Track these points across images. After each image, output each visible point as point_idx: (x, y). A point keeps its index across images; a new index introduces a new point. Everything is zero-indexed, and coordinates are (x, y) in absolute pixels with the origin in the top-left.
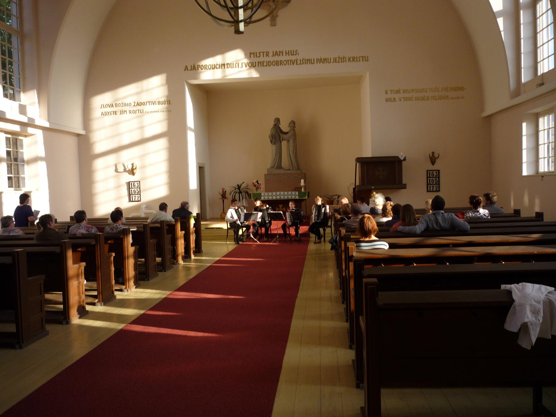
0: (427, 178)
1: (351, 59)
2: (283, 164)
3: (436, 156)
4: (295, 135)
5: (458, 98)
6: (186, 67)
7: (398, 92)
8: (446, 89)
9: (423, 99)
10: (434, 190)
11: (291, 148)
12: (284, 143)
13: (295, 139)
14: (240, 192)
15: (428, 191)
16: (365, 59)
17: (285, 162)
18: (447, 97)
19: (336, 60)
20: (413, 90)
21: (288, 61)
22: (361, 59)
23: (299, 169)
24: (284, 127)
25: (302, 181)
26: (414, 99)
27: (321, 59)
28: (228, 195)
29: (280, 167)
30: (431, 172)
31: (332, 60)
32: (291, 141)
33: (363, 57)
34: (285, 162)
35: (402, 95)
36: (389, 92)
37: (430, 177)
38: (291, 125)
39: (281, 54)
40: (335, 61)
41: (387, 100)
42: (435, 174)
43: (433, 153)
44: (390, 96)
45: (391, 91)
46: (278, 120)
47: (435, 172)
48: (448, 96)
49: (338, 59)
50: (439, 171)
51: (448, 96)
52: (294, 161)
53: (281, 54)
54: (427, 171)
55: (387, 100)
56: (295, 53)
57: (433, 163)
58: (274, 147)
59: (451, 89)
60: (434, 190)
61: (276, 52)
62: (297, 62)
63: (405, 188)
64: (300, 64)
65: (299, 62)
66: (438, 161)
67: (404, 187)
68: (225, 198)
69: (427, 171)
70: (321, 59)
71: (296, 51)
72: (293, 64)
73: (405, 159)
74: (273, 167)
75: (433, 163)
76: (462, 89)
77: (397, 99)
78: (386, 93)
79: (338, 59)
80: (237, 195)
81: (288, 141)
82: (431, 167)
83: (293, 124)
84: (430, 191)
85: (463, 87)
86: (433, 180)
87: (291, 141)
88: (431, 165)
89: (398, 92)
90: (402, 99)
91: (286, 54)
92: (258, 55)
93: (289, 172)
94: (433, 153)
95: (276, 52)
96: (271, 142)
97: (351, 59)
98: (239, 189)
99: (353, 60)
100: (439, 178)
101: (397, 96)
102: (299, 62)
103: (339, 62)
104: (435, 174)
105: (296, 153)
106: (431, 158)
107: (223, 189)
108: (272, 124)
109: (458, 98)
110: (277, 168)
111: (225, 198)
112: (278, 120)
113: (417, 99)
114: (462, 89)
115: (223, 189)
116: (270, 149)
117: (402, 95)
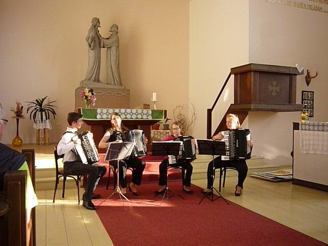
2: (102, 77)
3: (312, 75)
11: (113, 58)
14: (42, 110)
18: (319, 9)
23: (121, 85)
24: (104, 32)
29: (97, 80)
32: (114, 48)
38: (113, 29)
42: (310, 95)
46: (96, 23)
48: (321, 8)
50: (313, 92)
51: (321, 8)
52: (116, 75)
54: (303, 92)
57: (308, 83)
58: (92, 53)
68: (21, 117)
69: (303, 92)
75: (308, 83)
80: (39, 114)
82: (306, 88)
83: (115, 29)
87: (114, 48)
88: (306, 85)
93: (110, 87)
96: (90, 46)
98: (41, 105)
104: (310, 95)
105: (118, 64)
107: (18, 104)
108: (89, 25)
110: (94, 81)
111: (21, 117)
112: (96, 23)
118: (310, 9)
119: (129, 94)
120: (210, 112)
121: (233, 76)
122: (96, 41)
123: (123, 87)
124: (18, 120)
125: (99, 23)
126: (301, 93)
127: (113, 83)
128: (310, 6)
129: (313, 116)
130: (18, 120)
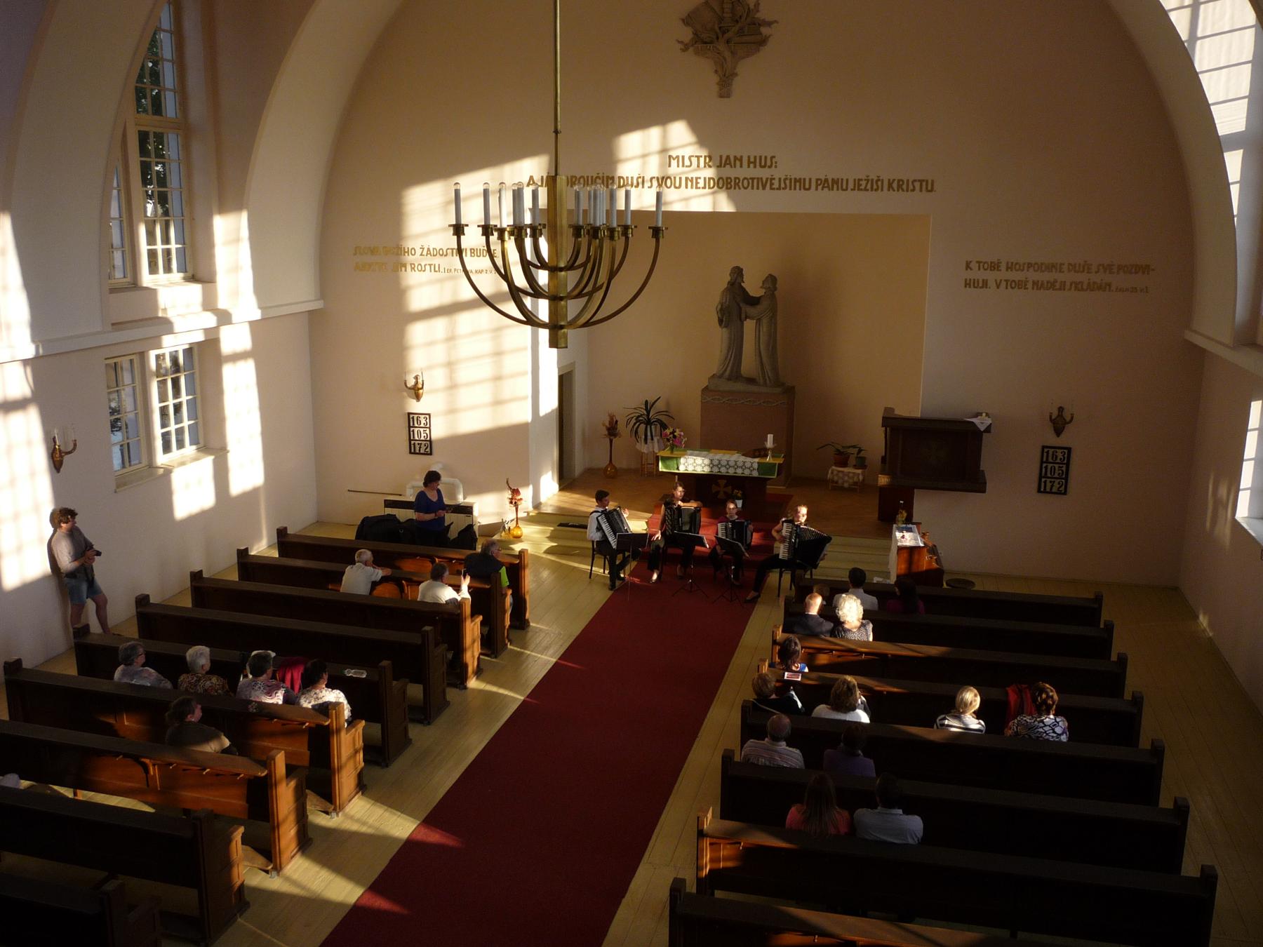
0: (1042, 462)
1: (895, 185)
4: (773, 310)
5: (1134, 290)
6: (531, 178)
7: (994, 266)
8: (1108, 268)
9: (1051, 285)
10: (1054, 490)
11: (763, 338)
12: (749, 325)
15: (1039, 491)
16: (927, 186)
17: (749, 364)
19: (860, 185)
20: (1030, 265)
21: (753, 179)
22: (917, 185)
24: (753, 286)
25: (770, 437)
26: (1030, 285)
27: (826, 180)
28: (621, 427)
30: (1051, 451)
31: (851, 185)
32: (765, 321)
33: (921, 181)
34: (749, 364)
35: (1003, 274)
36: (974, 265)
37: (1047, 462)
39: (738, 163)
40: (857, 186)
41: (967, 284)
43: (1061, 409)
44: (976, 274)
45: (979, 262)
46: (738, 272)
49: (863, 183)
50: (1069, 450)
51: (1110, 285)
52: (768, 367)
53: (738, 163)
54: (1044, 447)
55: (967, 284)
56: (769, 163)
57: (1058, 432)
59: (1120, 268)
60: (1054, 490)
61: (728, 157)
62: (772, 184)
64: (779, 189)
65: (776, 185)
66: (1069, 429)
68: (615, 435)
69: (1044, 447)
70: (826, 180)
71: (772, 157)
72: (764, 188)
73: (988, 430)
74: (721, 376)
75: (1058, 432)
76: (1145, 269)
77: (992, 283)
78: (968, 266)
79: (863, 183)
80: (643, 426)
81: (759, 321)
82: (1053, 440)
83: (771, 280)
84: (1045, 492)
85: (1148, 266)
86: (1053, 469)
87: (765, 321)
89: (994, 266)
90: (1004, 284)
91: (749, 163)
92: (687, 162)
95: (728, 157)
96: (721, 321)
97: (895, 185)
99: (900, 187)
100: (1068, 465)
101: (991, 276)
102: (776, 185)
103: (866, 190)
104: (1060, 456)
107: (612, 417)
109: (1134, 290)
110: (729, 379)
112: (738, 272)
113: (1037, 285)
114: (1145, 269)
115: (612, 417)
116: (718, 337)
117: (1003, 274)
118: (1076, 288)
122: (737, 304)
124: (611, 441)
125: (742, 276)
126: (1039, 450)
127: (762, 381)
128: (1076, 284)
129: (1065, 493)
130: (611, 441)
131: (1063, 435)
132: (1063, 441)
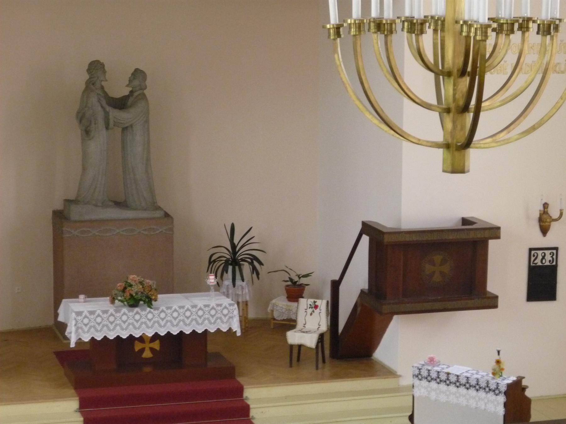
3: (554, 212)
13: (147, 121)
30: (540, 252)
43: (546, 205)
47: (548, 252)
50: (556, 249)
54: (531, 250)
57: (544, 231)
63: (495, 306)
66: (555, 228)
67: (491, 302)
69: (531, 250)
75: (544, 231)
82: (540, 241)
88: (539, 234)
94: (546, 205)
105: (148, 160)
106: (540, 220)
119: (172, 230)
120: (336, 285)
121: (365, 239)
123: (158, 214)
131: (549, 234)
132: (549, 241)
